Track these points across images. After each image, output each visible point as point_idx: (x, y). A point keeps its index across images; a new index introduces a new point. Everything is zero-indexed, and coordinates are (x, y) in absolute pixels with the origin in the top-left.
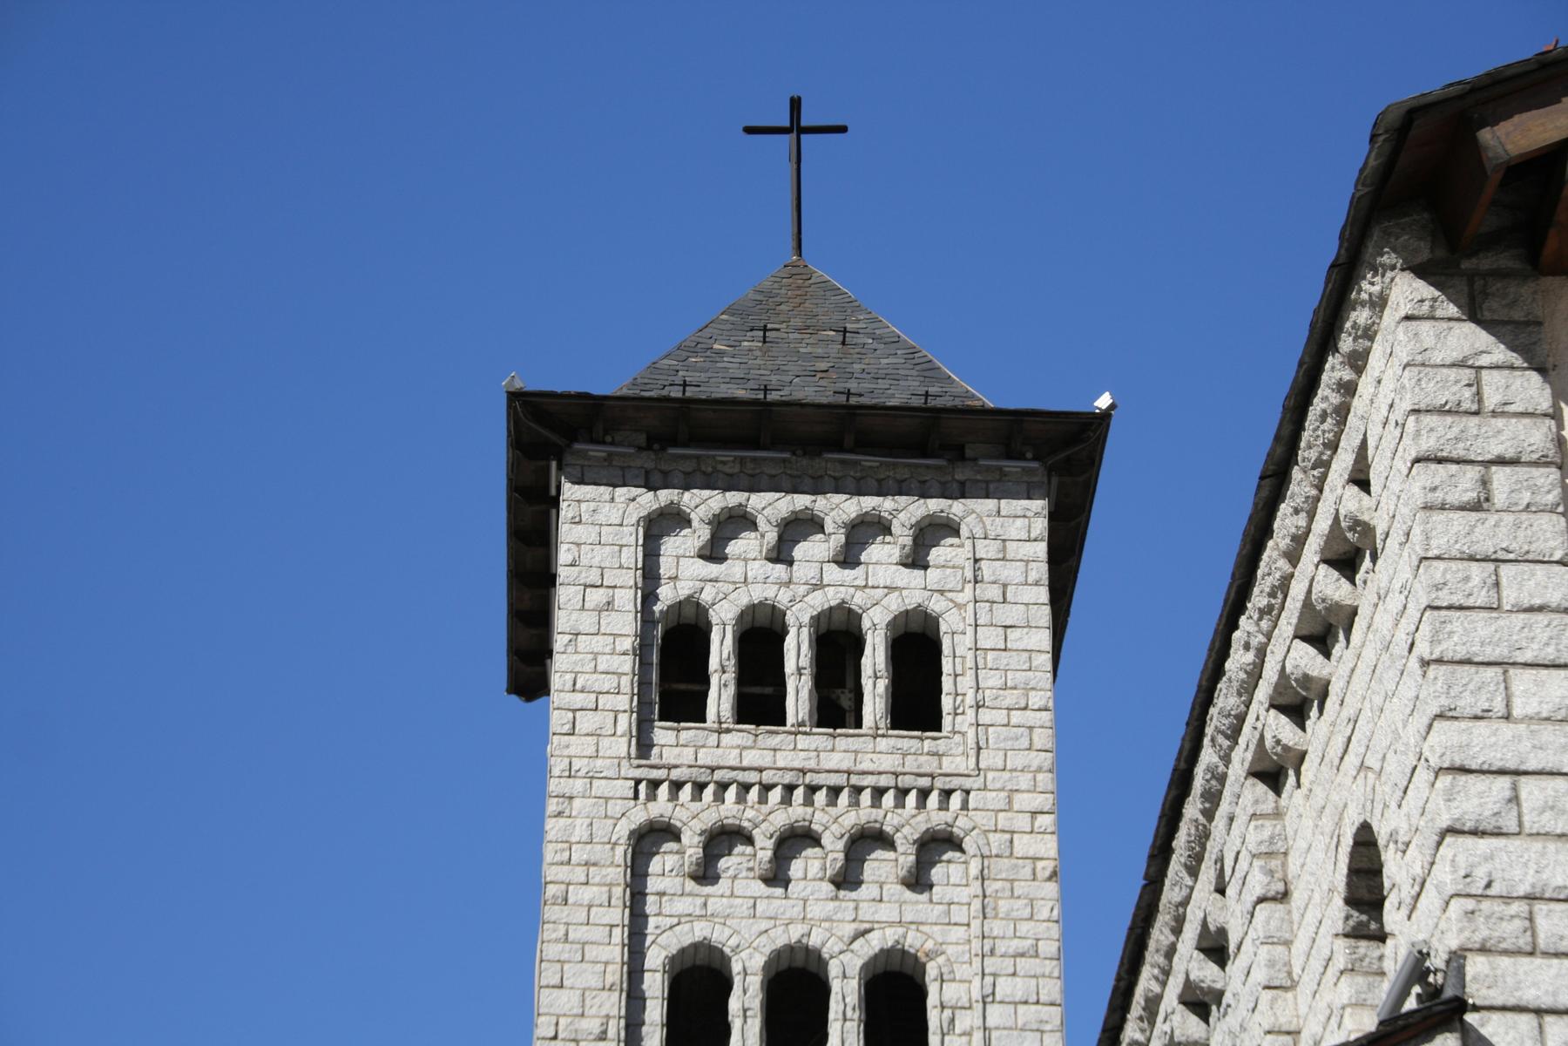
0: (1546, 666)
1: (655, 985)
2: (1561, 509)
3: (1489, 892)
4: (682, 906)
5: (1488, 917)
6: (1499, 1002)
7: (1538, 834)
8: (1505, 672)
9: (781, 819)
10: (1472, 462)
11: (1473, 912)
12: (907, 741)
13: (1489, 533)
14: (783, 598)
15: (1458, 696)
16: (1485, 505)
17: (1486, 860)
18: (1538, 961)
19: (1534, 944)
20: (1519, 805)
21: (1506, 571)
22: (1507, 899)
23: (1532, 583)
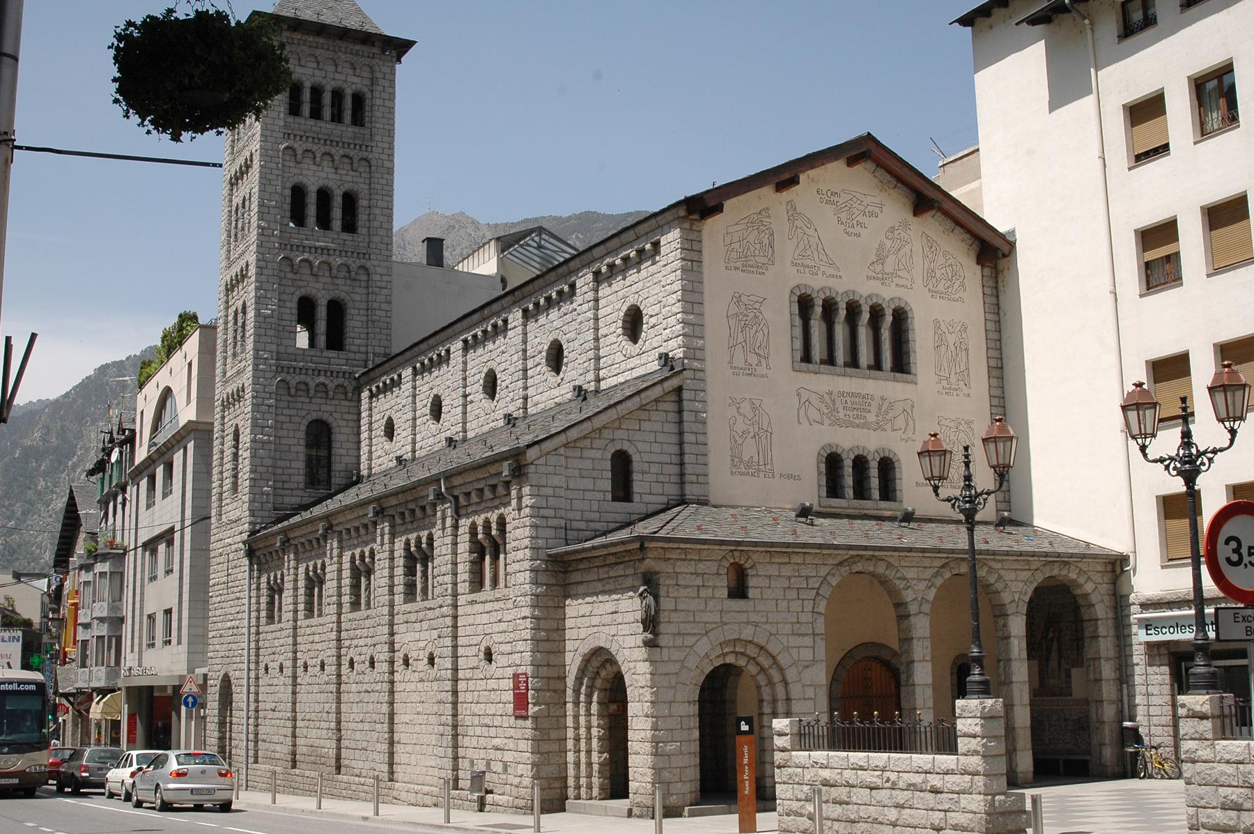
1: (288, 192)
4: (295, 171)
9: (323, 149)
12: (357, 129)
14: (324, 82)
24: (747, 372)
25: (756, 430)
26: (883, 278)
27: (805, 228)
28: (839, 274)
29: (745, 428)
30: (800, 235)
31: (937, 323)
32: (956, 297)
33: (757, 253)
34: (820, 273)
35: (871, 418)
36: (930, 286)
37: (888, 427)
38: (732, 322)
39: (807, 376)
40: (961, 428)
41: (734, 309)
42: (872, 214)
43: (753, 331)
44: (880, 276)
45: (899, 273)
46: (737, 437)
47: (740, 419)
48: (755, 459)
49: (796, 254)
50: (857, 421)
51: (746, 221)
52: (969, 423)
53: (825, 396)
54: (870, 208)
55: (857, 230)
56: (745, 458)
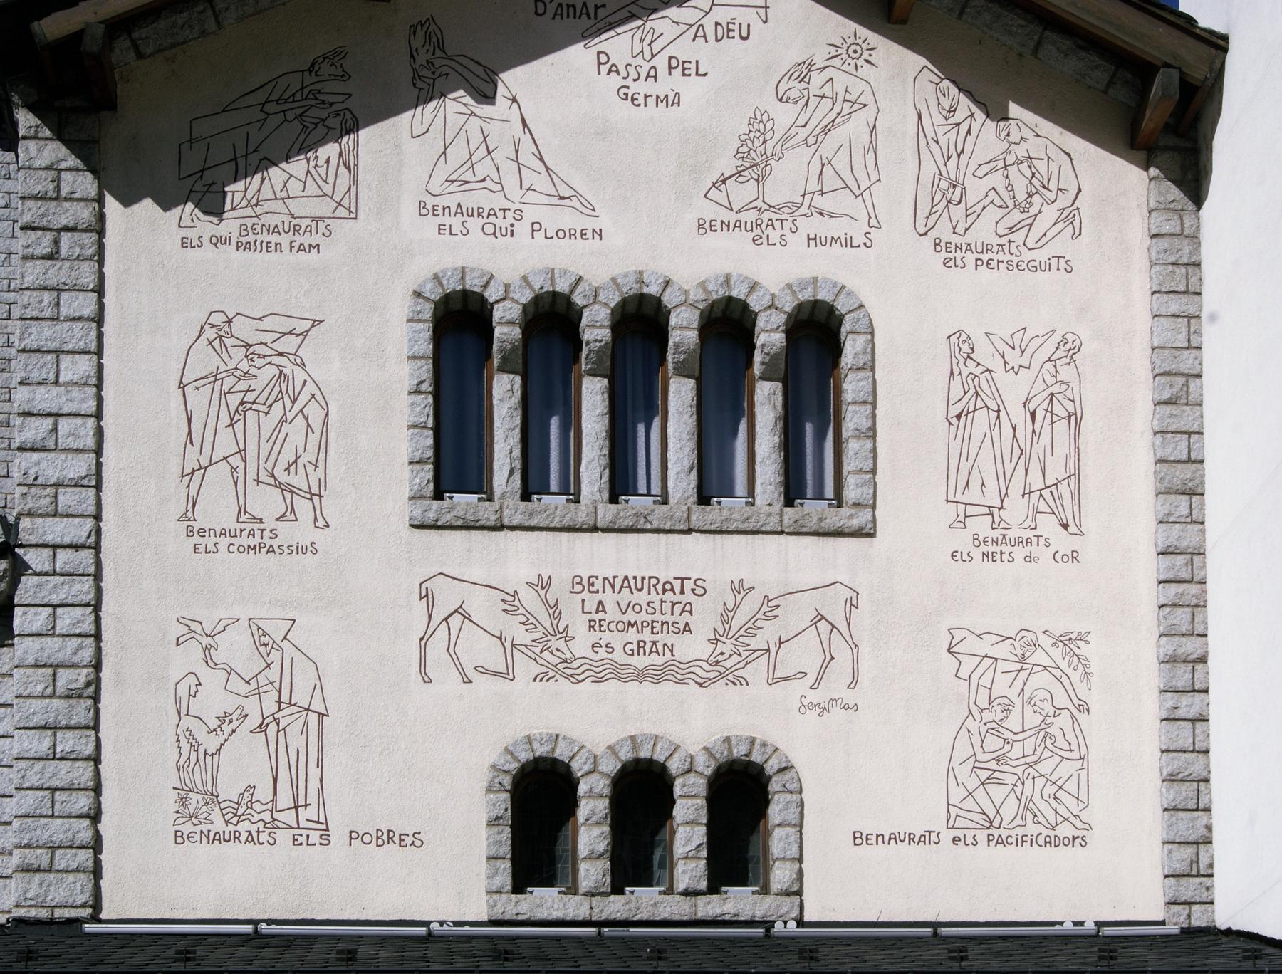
0: (79, 353)
2: (96, 258)
3: (36, 483)
5: (33, 497)
6: (34, 542)
7: (65, 449)
8: (58, 357)
10: (51, 230)
11: (26, 494)
15: (30, 372)
16: (56, 256)
17: (36, 464)
18: (56, 519)
19: (56, 510)
20: (57, 433)
21: (64, 296)
22: (45, 486)
23: (76, 303)
24: (245, 541)
25: (270, 706)
28: (591, 224)
29: (230, 704)
32: (1042, 255)
33: (295, 188)
34: (523, 228)
35: (693, 648)
38: (198, 400)
41: (206, 358)
42: (726, 32)
43: (269, 422)
44: (750, 216)
45: (819, 202)
46: (201, 734)
47: (211, 680)
49: (439, 177)
50: (640, 661)
51: (260, 97)
53: (530, 599)
55: (665, 85)
56: (229, 789)
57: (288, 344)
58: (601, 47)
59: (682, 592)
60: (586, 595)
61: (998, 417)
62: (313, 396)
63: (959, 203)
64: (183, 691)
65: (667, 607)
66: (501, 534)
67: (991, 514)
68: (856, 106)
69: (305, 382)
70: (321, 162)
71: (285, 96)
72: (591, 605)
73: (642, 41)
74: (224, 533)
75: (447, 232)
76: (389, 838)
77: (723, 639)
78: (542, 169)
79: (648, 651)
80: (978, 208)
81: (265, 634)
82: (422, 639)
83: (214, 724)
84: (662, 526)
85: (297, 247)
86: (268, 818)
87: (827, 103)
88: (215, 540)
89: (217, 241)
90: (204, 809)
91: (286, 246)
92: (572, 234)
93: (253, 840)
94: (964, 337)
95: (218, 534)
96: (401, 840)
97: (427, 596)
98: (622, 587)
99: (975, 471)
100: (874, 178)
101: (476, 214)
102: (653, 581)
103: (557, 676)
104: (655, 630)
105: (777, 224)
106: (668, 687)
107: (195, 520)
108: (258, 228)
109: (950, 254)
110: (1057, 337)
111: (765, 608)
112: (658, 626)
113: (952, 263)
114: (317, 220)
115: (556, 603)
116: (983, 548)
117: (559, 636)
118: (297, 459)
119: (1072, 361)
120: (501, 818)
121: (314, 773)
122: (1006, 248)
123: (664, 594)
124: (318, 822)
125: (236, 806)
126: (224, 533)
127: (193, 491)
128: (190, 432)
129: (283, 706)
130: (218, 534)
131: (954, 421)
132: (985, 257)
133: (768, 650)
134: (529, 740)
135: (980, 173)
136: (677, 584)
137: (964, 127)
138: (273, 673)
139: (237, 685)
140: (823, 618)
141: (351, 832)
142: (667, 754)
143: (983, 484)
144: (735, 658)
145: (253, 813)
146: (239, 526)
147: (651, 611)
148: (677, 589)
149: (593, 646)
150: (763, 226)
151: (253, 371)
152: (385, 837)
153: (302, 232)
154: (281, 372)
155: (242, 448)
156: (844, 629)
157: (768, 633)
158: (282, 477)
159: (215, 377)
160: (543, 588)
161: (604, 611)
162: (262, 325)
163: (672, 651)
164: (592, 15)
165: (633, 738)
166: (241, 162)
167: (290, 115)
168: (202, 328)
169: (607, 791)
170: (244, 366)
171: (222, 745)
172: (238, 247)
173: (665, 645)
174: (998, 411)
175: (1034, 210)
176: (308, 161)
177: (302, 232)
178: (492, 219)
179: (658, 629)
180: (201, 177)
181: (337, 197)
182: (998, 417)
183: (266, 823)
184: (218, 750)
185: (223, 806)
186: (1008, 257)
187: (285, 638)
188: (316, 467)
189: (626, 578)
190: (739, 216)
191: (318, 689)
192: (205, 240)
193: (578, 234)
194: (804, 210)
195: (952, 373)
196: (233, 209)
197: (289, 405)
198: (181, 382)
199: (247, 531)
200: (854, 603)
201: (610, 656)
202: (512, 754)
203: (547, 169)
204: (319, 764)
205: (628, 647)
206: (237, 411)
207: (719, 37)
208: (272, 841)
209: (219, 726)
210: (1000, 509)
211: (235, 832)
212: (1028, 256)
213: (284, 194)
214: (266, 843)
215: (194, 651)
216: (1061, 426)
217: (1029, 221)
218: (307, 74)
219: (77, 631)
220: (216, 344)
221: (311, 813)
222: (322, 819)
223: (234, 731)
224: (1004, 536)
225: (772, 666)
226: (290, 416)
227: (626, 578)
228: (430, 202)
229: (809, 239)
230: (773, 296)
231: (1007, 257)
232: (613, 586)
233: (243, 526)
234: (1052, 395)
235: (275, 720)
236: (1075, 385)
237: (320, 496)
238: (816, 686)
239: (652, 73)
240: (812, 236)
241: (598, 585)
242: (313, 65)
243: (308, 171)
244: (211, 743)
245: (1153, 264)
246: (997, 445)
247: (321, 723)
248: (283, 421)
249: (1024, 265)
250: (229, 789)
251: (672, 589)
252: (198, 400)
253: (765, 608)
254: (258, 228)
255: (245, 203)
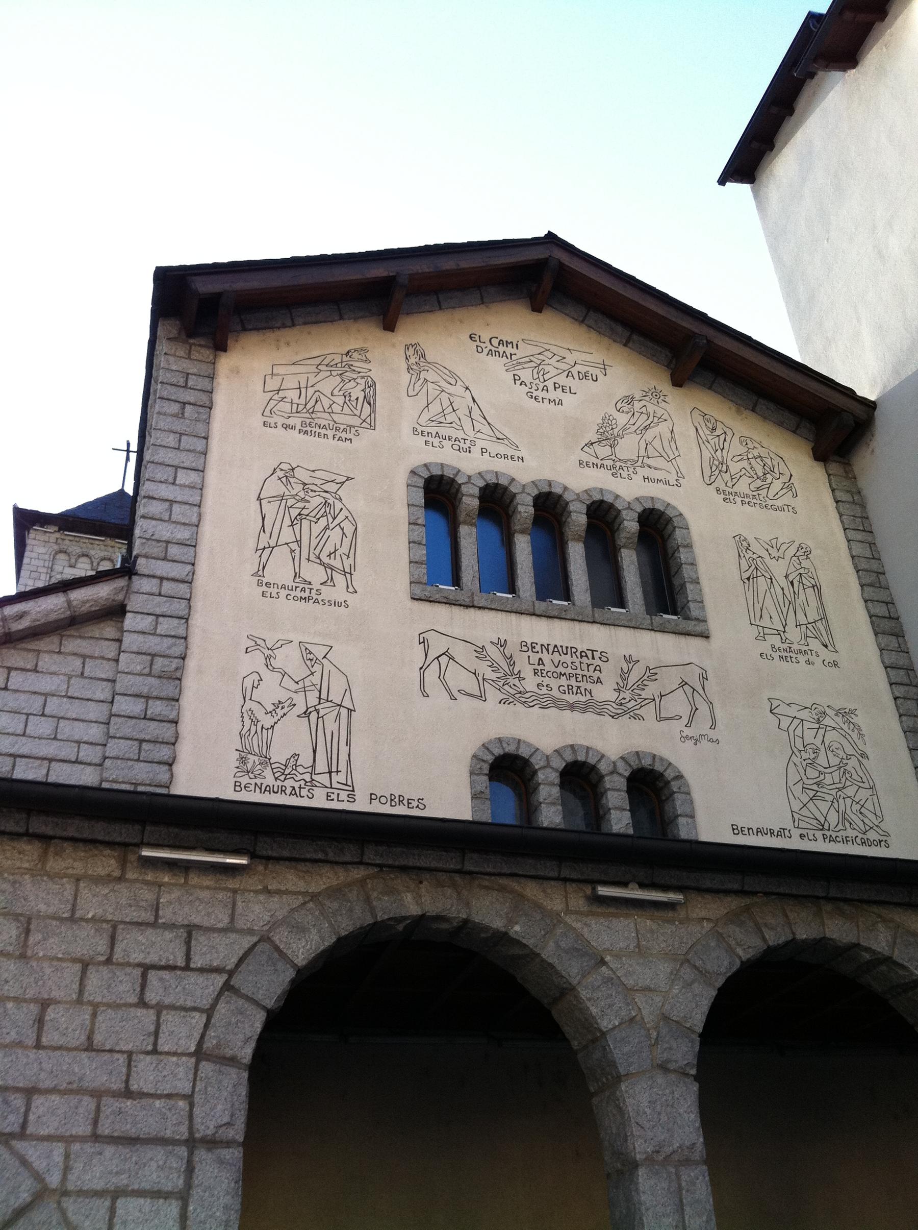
0: (191, 469)
13: (179, 426)
24: (298, 593)
25: (313, 700)
26: (616, 468)
27: (443, 384)
28: (517, 454)
29: (283, 696)
30: (433, 393)
31: (742, 545)
32: (779, 503)
34: (476, 450)
35: (605, 693)
36: (720, 483)
37: (648, 711)
38: (270, 509)
39: (442, 611)
40: (827, 721)
41: (275, 487)
43: (317, 528)
44: (610, 463)
46: (260, 714)
48: (306, 759)
50: (571, 698)
51: (317, 361)
52: (845, 714)
53: (493, 652)
54: (578, 368)
55: (553, 395)
56: (279, 755)
57: (332, 487)
58: (515, 372)
59: (593, 658)
60: (530, 653)
61: (772, 582)
62: (347, 517)
63: (726, 472)
64: (248, 683)
65: (584, 667)
66: (472, 610)
67: (779, 634)
68: (660, 420)
69: (342, 509)
70: (353, 398)
71: (331, 364)
72: (534, 658)
73: (538, 373)
74: (283, 587)
75: (431, 445)
76: (400, 801)
77: (624, 690)
78: (486, 424)
79: (575, 692)
80: (738, 476)
81: (310, 653)
82: (421, 668)
83: (270, 708)
84: (576, 618)
85: (337, 439)
86: (307, 777)
87: (645, 417)
88: (278, 591)
89: (286, 427)
90: (259, 767)
91: (330, 436)
92: (506, 457)
93: (296, 794)
94: (742, 538)
95: (280, 587)
96: (409, 803)
97: (424, 642)
98: (554, 651)
99: (764, 609)
100: (677, 454)
101: (447, 438)
102: (574, 650)
103: (515, 702)
104: (578, 680)
105: (625, 469)
106: (590, 716)
107: (264, 577)
108: (313, 425)
109: (728, 497)
110: (796, 545)
111: (648, 674)
112: (580, 678)
113: (728, 500)
114: (351, 426)
115: (511, 656)
116: (778, 653)
117: (514, 676)
118: (336, 551)
119: (808, 558)
120: (482, 792)
121: (344, 749)
122: (757, 497)
123: (581, 658)
124: (346, 785)
125: (284, 768)
126: (283, 587)
127: (264, 560)
128: (263, 525)
129: (322, 701)
130: (280, 587)
131: (746, 581)
132: (747, 500)
133: (654, 700)
134: (500, 740)
135: (736, 459)
136: (589, 654)
137: (722, 438)
138: (316, 679)
139: (287, 682)
140: (686, 683)
141: (371, 794)
142: (597, 759)
143: (771, 617)
144: (633, 703)
145: (297, 774)
146: (295, 585)
147: (574, 667)
148: (590, 656)
149: (538, 685)
150: (617, 468)
151: (308, 498)
152: (397, 800)
153: (341, 431)
154: (326, 501)
155: (299, 539)
156: (701, 692)
157: (652, 690)
158: (326, 560)
159: (282, 497)
160: (501, 646)
161: (543, 664)
162: (314, 474)
163: (590, 693)
164: (509, 357)
165: (572, 746)
166: (303, 391)
167: (334, 373)
168: (275, 470)
169: (557, 781)
170: (302, 494)
171: (275, 723)
172: (300, 433)
173: (586, 689)
174: (771, 579)
175: (769, 481)
176: (345, 397)
177: (341, 431)
178: (457, 443)
179: (580, 678)
180: (278, 393)
181: (363, 417)
182: (772, 582)
183: (306, 782)
184: (272, 727)
185: (273, 766)
186: (759, 502)
187: (325, 657)
188: (348, 557)
189: (556, 646)
190: (605, 462)
191: (348, 692)
192: (279, 425)
193: (509, 457)
194: (639, 463)
195: (739, 556)
196: (297, 412)
197: (331, 520)
198: (259, 497)
199: (300, 589)
200: (705, 676)
201: (550, 692)
202: (488, 749)
203: (489, 424)
204: (348, 743)
205: (561, 688)
206: (296, 518)
207: (581, 378)
208: (310, 796)
209: (274, 710)
210: (784, 632)
211: (282, 786)
212: (770, 503)
213: (330, 410)
214: (306, 797)
215: (257, 661)
216: (810, 591)
217: (768, 486)
218: (344, 356)
219: (173, 634)
220: (284, 480)
221: (341, 778)
222: (349, 783)
223: (285, 715)
224: (790, 648)
225: (658, 710)
226: (331, 526)
227: (556, 646)
228: (420, 429)
229: (644, 478)
230: (629, 503)
231: (759, 502)
232: (548, 650)
233: (297, 585)
234: (801, 574)
235: (316, 710)
236: (812, 570)
237: (351, 574)
238: (689, 725)
239: (545, 388)
240: (646, 477)
241: (538, 648)
242: (348, 352)
243: (345, 402)
244: (267, 721)
245: (841, 515)
246: (774, 597)
247: (349, 716)
248: (326, 528)
249: (769, 507)
250: (279, 755)
251: (586, 656)
252: (270, 509)
253: (648, 674)
254: (313, 425)
255: (305, 410)
